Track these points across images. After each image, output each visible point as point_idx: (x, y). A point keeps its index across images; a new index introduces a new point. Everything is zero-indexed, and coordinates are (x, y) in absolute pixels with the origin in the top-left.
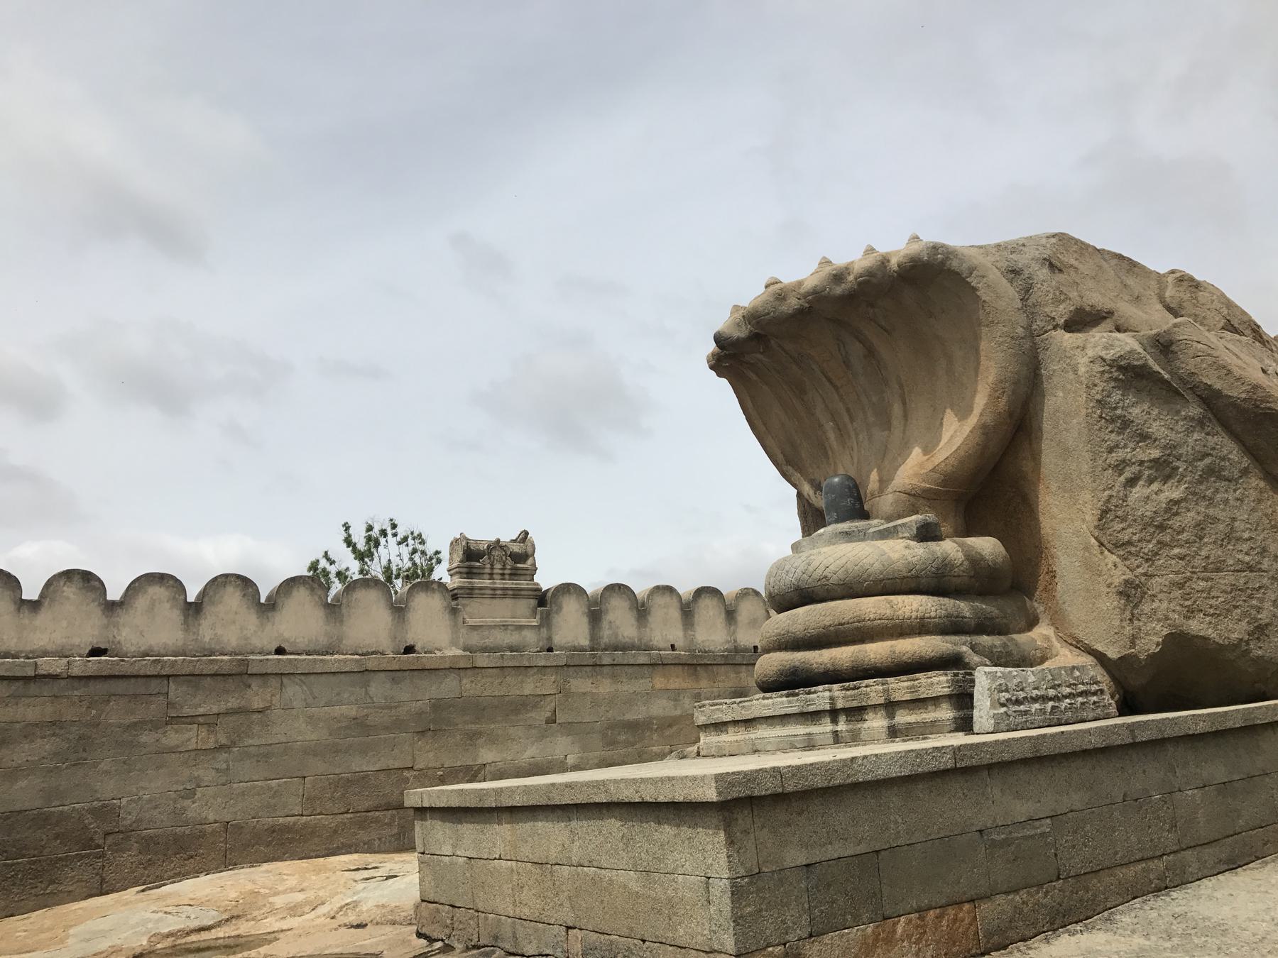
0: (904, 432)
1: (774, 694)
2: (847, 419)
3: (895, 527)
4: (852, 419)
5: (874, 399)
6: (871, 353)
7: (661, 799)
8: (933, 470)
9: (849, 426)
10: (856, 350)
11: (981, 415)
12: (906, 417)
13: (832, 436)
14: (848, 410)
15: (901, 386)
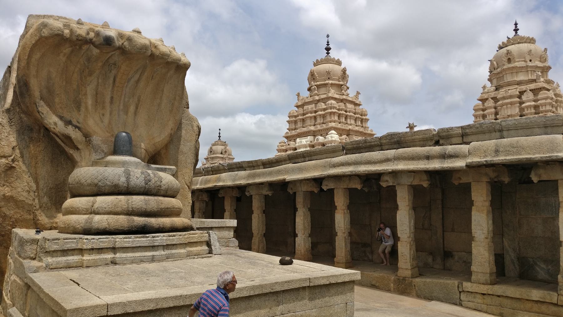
0: (134, 120)
1: (133, 236)
2: (108, 99)
3: (166, 168)
4: (112, 102)
5: (126, 100)
6: (138, 81)
7: (339, 281)
8: (154, 145)
9: (108, 105)
10: (137, 77)
11: (172, 129)
12: (136, 113)
13: (90, 102)
14: (112, 98)
15: (139, 101)
